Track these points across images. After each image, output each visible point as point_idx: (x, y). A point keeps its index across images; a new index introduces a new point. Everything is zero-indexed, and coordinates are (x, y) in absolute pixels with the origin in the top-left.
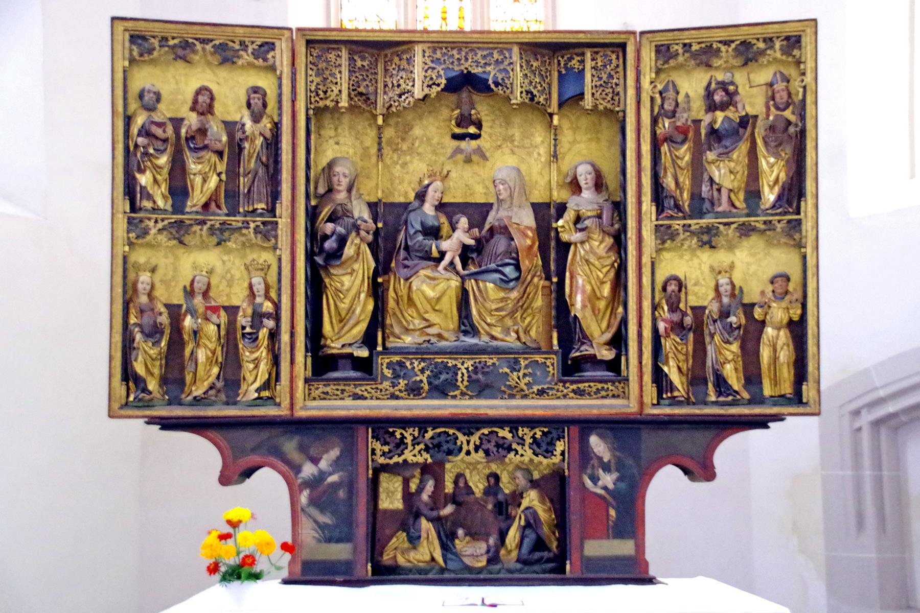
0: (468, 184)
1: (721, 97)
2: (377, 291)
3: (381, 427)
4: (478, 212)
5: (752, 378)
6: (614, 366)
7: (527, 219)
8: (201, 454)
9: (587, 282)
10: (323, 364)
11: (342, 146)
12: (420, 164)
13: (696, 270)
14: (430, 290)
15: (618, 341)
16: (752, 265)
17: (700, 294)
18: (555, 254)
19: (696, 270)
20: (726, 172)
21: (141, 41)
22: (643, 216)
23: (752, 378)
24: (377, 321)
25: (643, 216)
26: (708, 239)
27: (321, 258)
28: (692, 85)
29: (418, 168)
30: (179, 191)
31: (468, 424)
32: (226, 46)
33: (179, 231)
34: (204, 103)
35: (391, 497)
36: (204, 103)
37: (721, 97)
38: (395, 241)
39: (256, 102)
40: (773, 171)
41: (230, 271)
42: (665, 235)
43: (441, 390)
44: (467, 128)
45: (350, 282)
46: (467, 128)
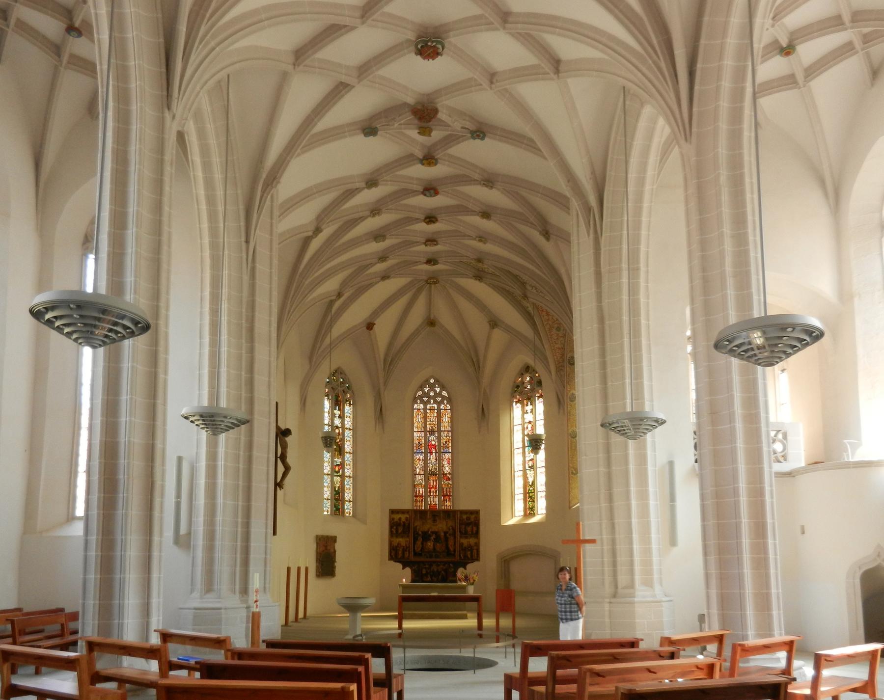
0: (435, 529)
1: (468, 518)
2: (422, 544)
3: (423, 562)
4: (436, 533)
5: (472, 556)
6: (454, 555)
7: (442, 534)
8: (400, 566)
9: (451, 542)
10: (415, 554)
11: (418, 523)
12: (428, 526)
13: (465, 542)
14: (430, 545)
15: (454, 551)
16: (472, 541)
17: (465, 545)
18: (446, 539)
19: (465, 542)
20: (469, 529)
21: (392, 512)
22: (458, 534)
23: (472, 556)
24: (422, 548)
25: (458, 534)
26: (466, 538)
27: (415, 539)
28: (465, 517)
29: (428, 526)
30: (397, 531)
31: (434, 562)
32: (403, 512)
33: (397, 537)
34: (400, 519)
35: (424, 572)
36: (400, 519)
37: (468, 518)
38: (426, 536)
39: (407, 519)
40: (475, 529)
41: (402, 541)
42: (461, 537)
43: (431, 557)
44: (435, 521)
45: (419, 543)
46: (435, 521)
